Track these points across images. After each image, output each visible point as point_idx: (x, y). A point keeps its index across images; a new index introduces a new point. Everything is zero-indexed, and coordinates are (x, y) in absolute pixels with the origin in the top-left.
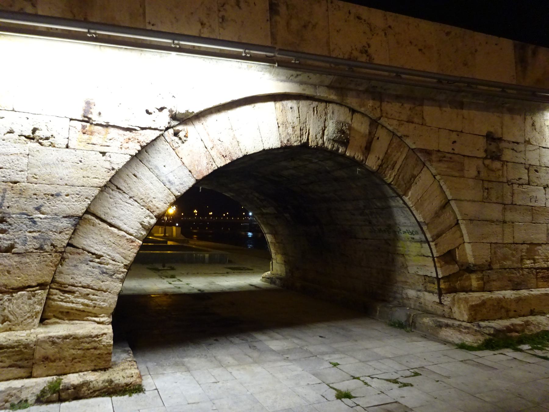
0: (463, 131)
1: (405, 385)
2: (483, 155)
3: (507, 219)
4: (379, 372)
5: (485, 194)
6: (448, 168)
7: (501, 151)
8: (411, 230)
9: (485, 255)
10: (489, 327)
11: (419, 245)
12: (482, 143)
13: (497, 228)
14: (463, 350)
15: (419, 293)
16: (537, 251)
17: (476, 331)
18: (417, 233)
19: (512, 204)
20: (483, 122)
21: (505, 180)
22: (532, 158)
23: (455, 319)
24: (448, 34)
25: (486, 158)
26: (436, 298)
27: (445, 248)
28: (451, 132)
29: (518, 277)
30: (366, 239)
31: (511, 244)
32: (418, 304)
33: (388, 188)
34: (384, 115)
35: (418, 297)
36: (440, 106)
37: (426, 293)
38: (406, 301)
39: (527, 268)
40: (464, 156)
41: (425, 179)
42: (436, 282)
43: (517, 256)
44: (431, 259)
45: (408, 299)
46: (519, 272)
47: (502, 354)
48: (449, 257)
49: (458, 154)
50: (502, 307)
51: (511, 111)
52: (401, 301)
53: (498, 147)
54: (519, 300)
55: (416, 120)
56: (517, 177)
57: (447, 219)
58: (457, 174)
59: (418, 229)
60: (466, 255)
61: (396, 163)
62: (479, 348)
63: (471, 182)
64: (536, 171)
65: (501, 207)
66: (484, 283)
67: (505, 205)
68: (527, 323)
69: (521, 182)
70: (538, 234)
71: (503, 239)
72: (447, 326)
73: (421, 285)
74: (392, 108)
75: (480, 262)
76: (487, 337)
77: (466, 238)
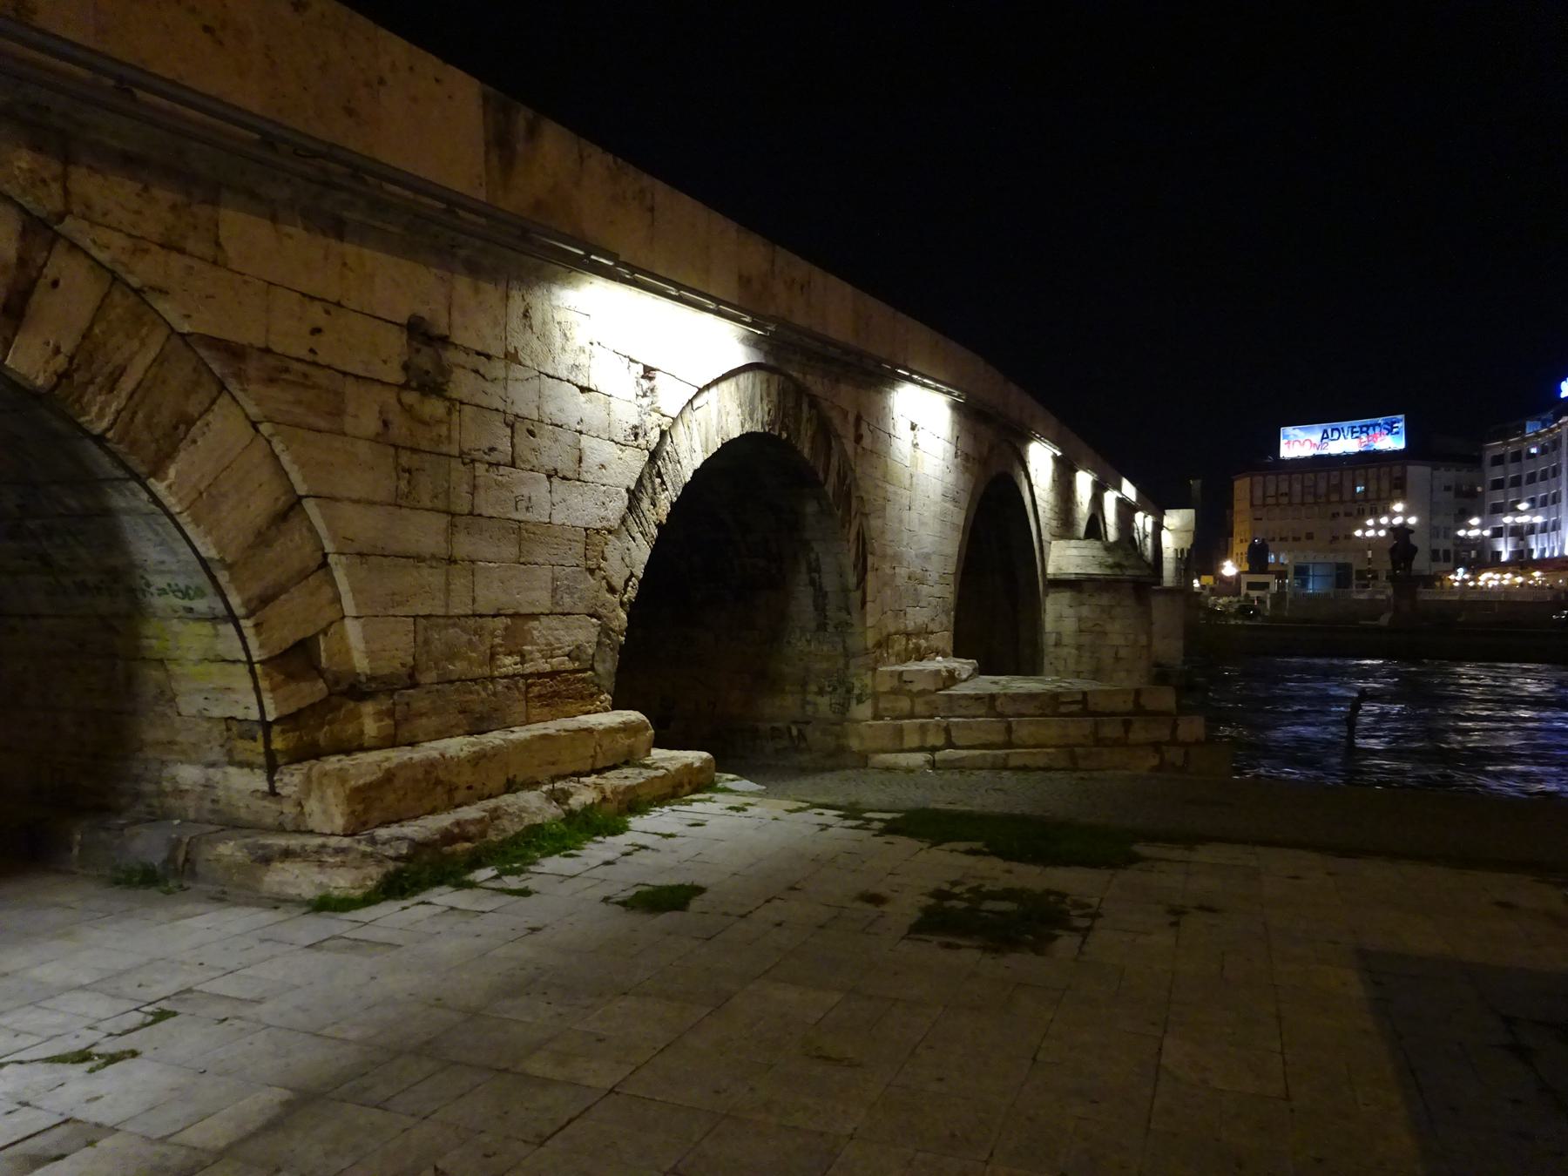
0: (344, 302)
1: (113, 1059)
2: (398, 377)
4: (36, 1040)
5: (403, 485)
6: (299, 402)
7: (445, 371)
8: (182, 586)
9: (399, 648)
10: (398, 839)
11: (206, 629)
12: (395, 343)
13: (433, 577)
14: (325, 913)
15: (211, 771)
16: (529, 632)
17: (364, 855)
18: (200, 593)
19: (471, 514)
20: (396, 285)
21: (456, 452)
23: (311, 832)
25: (405, 387)
26: (259, 782)
27: (286, 635)
28: (306, 300)
29: (482, 702)
30: (36, 616)
31: (467, 616)
32: (208, 805)
33: (94, 449)
34: (77, 208)
35: (209, 785)
36: (274, 219)
37: (232, 770)
38: (171, 802)
39: (506, 677)
40: (345, 374)
41: (223, 429)
42: (260, 735)
43: (482, 648)
44: (242, 669)
45: (180, 793)
46: (485, 689)
47: (423, 903)
48: (297, 660)
49: (329, 367)
50: (438, 782)
51: (474, 269)
52: (155, 802)
53: (438, 362)
54: (478, 759)
55: (190, 245)
56: (485, 446)
57: (292, 549)
58: (322, 424)
59: (202, 579)
60: (348, 651)
61: (122, 370)
62: (368, 901)
63: (363, 449)
64: (532, 433)
65: (444, 520)
66: (397, 725)
67: (453, 515)
68: (495, 814)
69: (494, 457)
72: (287, 854)
73: (217, 749)
74: (109, 193)
75: (384, 669)
76: (391, 866)
77: (349, 605)
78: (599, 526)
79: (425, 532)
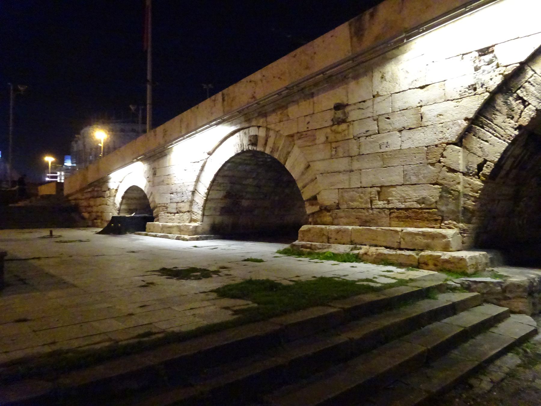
2: (331, 123)
3: (354, 168)
5: (333, 153)
12: (329, 115)
16: (390, 192)
19: (359, 155)
22: (382, 107)
24: (294, 57)
25: (333, 125)
29: (366, 216)
31: (358, 188)
36: (298, 104)
39: (379, 208)
41: (296, 152)
43: (365, 198)
46: (368, 212)
50: (324, 235)
54: (338, 231)
56: (364, 131)
58: (310, 144)
61: (278, 147)
63: (321, 146)
64: (388, 118)
65: (347, 160)
66: (333, 219)
67: (351, 157)
70: (391, 176)
71: (350, 185)
74: (273, 118)
78: (436, 143)
79: (342, 164)
